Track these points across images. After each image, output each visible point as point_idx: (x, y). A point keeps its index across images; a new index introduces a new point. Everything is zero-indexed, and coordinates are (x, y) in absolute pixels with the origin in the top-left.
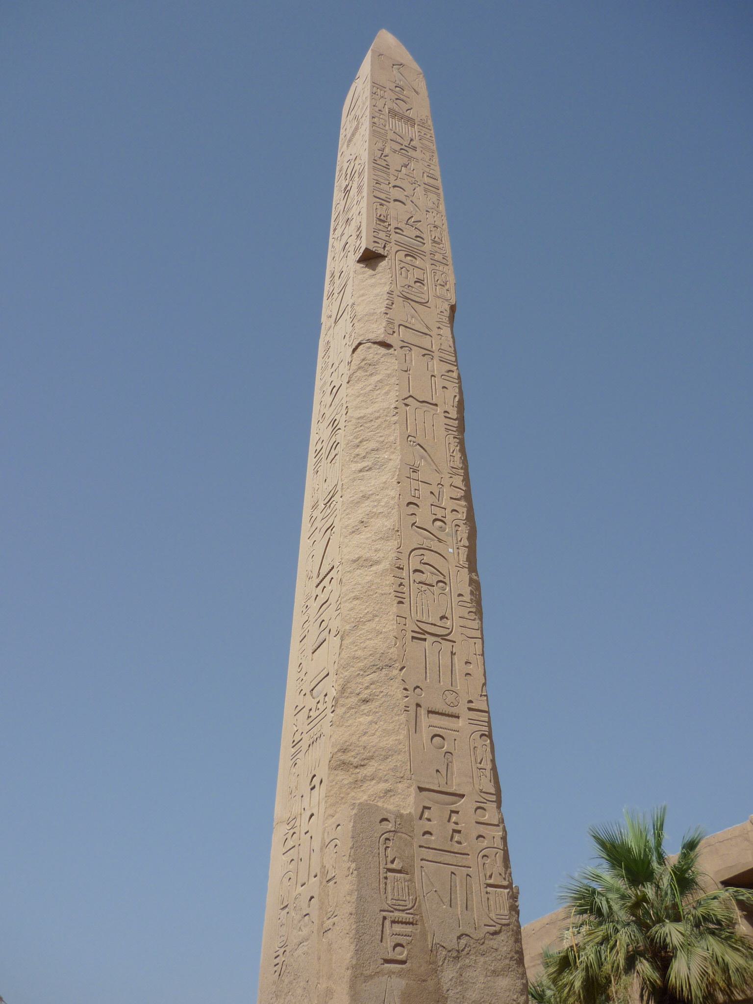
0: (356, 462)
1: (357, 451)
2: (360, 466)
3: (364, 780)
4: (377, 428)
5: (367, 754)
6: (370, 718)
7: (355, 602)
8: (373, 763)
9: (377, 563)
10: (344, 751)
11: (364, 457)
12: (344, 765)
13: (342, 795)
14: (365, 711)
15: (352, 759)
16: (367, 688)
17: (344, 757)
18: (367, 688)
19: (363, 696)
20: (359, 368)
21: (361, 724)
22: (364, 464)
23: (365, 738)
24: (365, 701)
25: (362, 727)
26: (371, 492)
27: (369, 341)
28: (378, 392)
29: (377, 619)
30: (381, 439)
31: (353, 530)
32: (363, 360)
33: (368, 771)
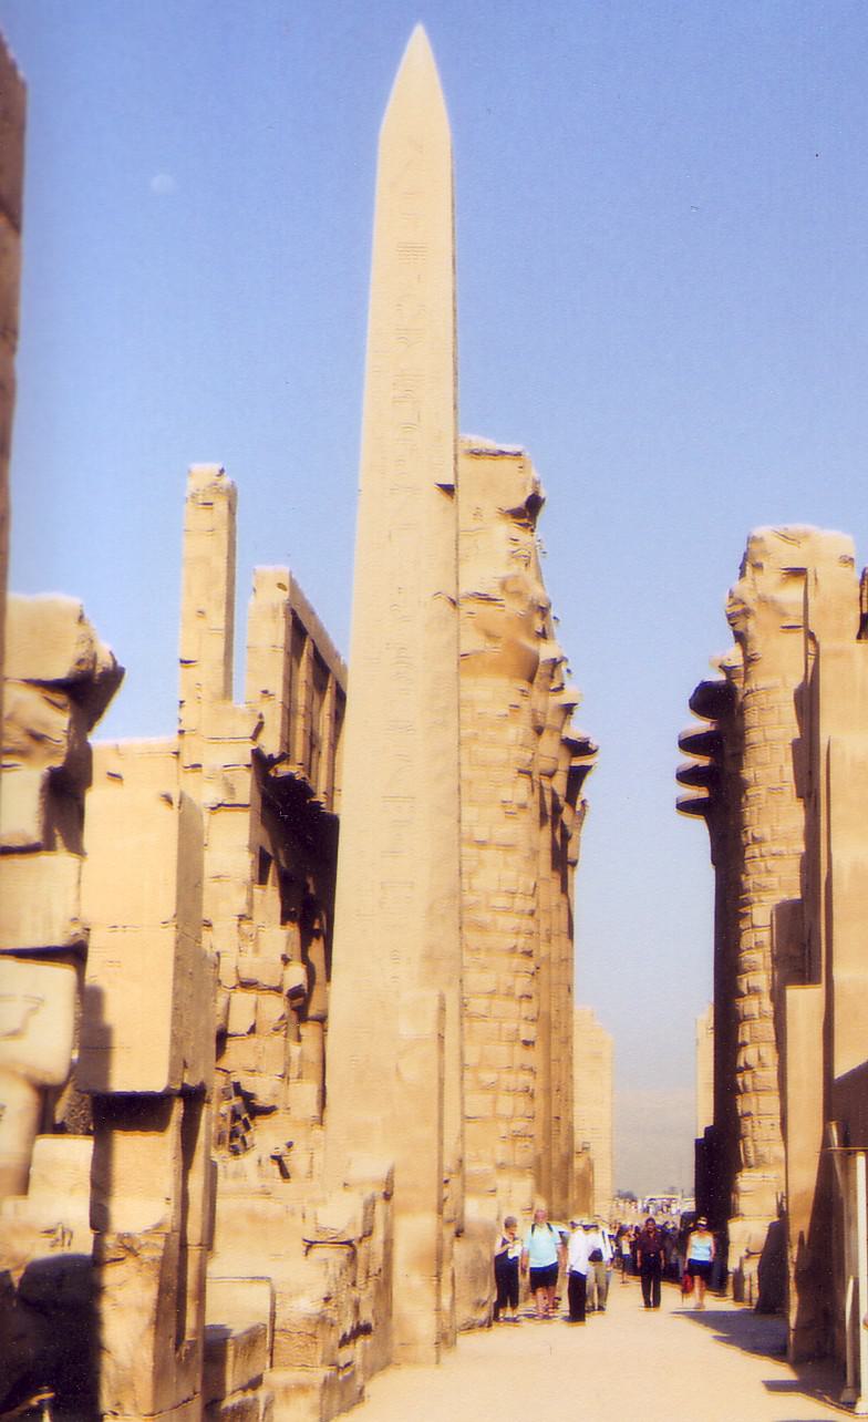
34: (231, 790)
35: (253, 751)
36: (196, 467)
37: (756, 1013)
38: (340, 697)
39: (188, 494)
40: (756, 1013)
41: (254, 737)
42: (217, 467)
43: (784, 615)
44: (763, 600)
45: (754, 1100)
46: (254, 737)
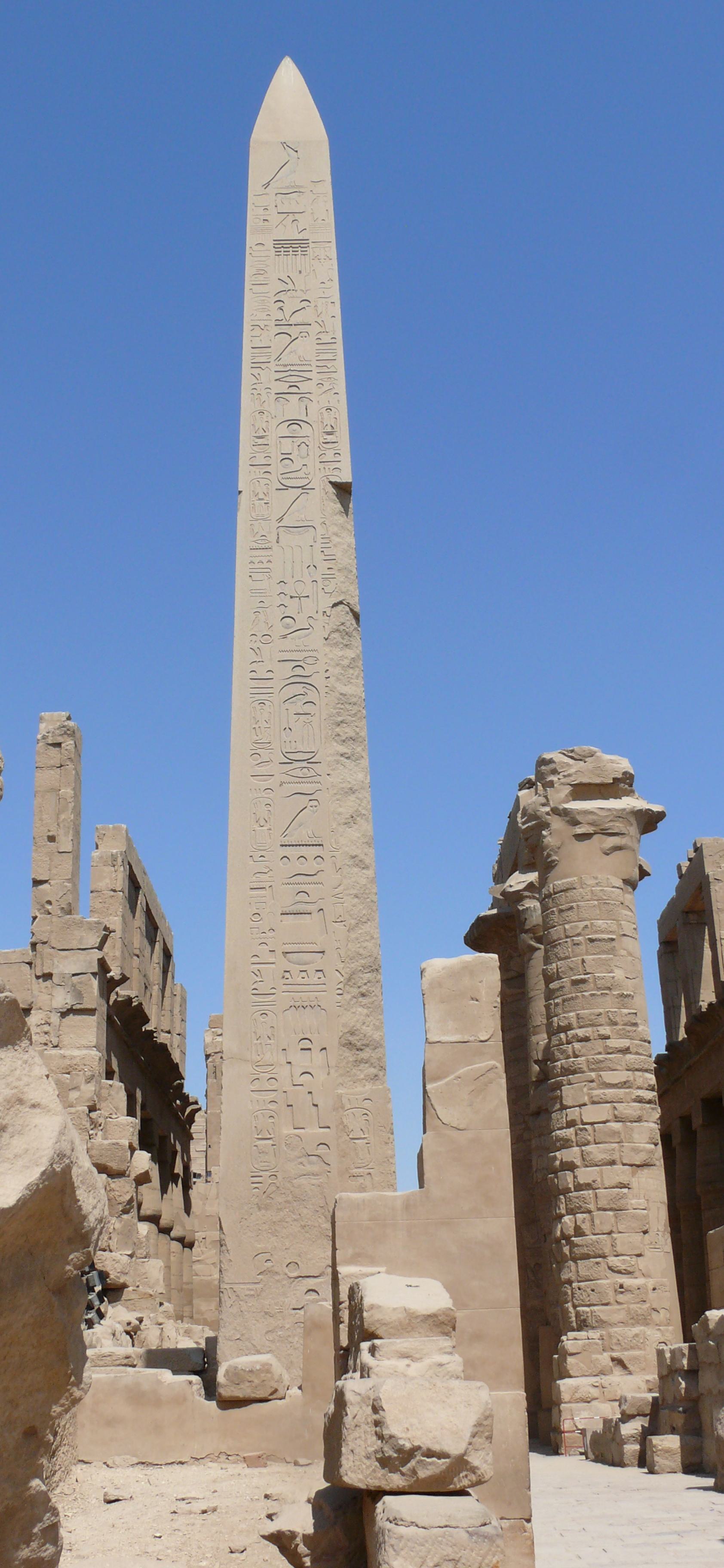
0: (337, 742)
1: (338, 730)
2: (342, 749)
3: (362, 1061)
4: (355, 715)
5: (364, 1042)
6: (365, 1011)
7: (356, 900)
8: (367, 1049)
9: (366, 867)
10: (352, 1033)
11: (344, 741)
12: (350, 1045)
13: (348, 1070)
14: (363, 1004)
15: (356, 1042)
16: (365, 984)
17: (351, 1038)
18: (365, 984)
19: (363, 989)
20: (338, 630)
21: (361, 1014)
22: (346, 750)
23: (364, 1027)
24: (363, 995)
25: (362, 1018)
26: (355, 788)
27: (348, 605)
28: (351, 671)
29: (369, 923)
30: (358, 730)
31: (346, 821)
32: (343, 624)
33: (364, 1055)
34: (79, 995)
35: (99, 960)
36: (45, 715)
37: (571, 1186)
38: (167, 955)
39: (39, 737)
40: (571, 1186)
41: (100, 948)
42: (64, 714)
43: (575, 823)
44: (555, 811)
45: (573, 1268)
46: (100, 948)
